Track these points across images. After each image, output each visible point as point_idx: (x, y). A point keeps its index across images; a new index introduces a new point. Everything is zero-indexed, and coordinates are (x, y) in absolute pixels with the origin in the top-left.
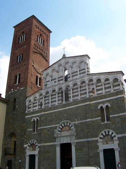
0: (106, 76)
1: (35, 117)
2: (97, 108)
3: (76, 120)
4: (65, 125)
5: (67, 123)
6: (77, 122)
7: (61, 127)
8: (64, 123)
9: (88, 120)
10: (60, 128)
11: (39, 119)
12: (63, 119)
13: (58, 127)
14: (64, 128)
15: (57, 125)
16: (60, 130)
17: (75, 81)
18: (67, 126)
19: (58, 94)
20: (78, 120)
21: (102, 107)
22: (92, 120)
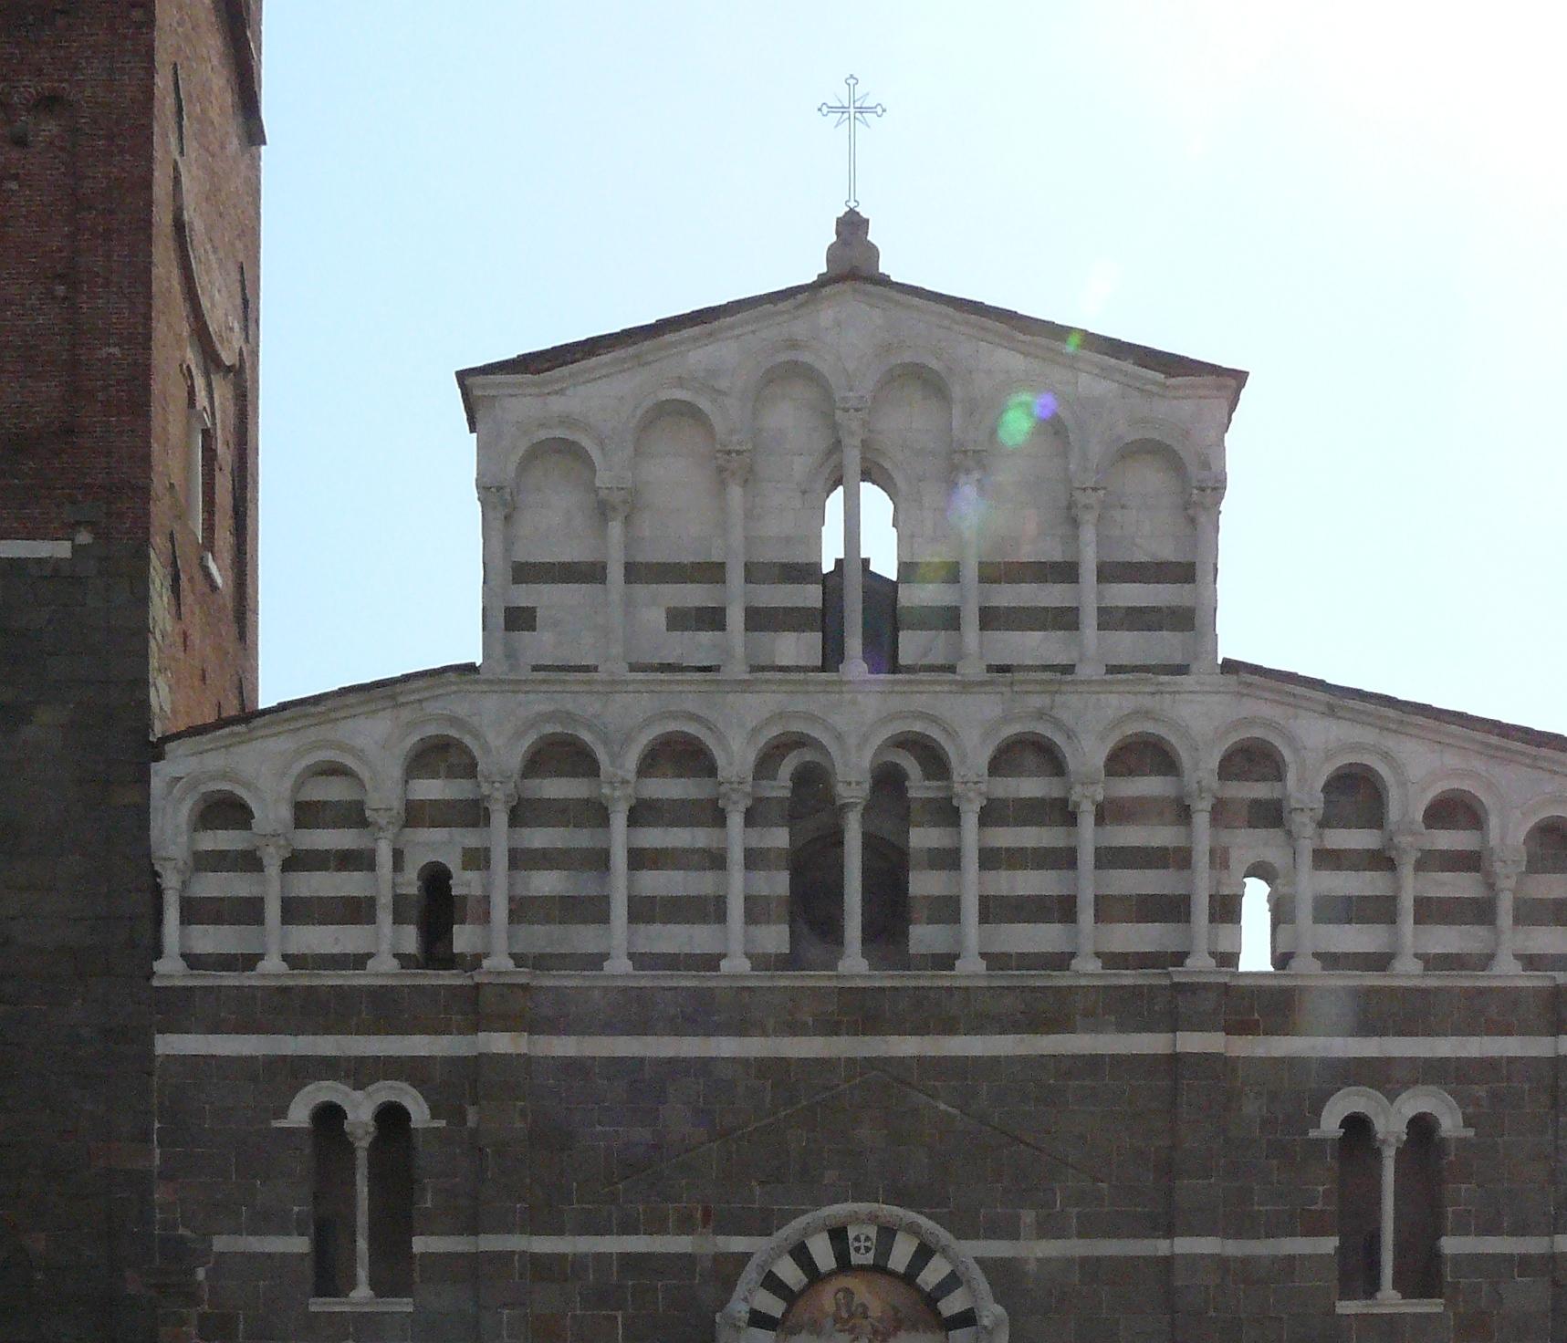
0: (1452, 760)
1: (360, 1072)
2: (1313, 1134)
3: (1028, 1217)
4: (856, 1259)
5: (887, 1234)
6: (1037, 1250)
7: (789, 1272)
8: (838, 1235)
9: (1185, 1245)
10: (772, 1283)
11: (419, 1113)
12: (830, 1176)
13: (751, 1274)
14: (828, 1298)
15: (738, 1244)
16: (774, 1306)
17: (1037, 701)
18: (879, 1268)
19: (752, 818)
20: (1048, 1229)
21: (1357, 1126)
22: (1233, 1248)
